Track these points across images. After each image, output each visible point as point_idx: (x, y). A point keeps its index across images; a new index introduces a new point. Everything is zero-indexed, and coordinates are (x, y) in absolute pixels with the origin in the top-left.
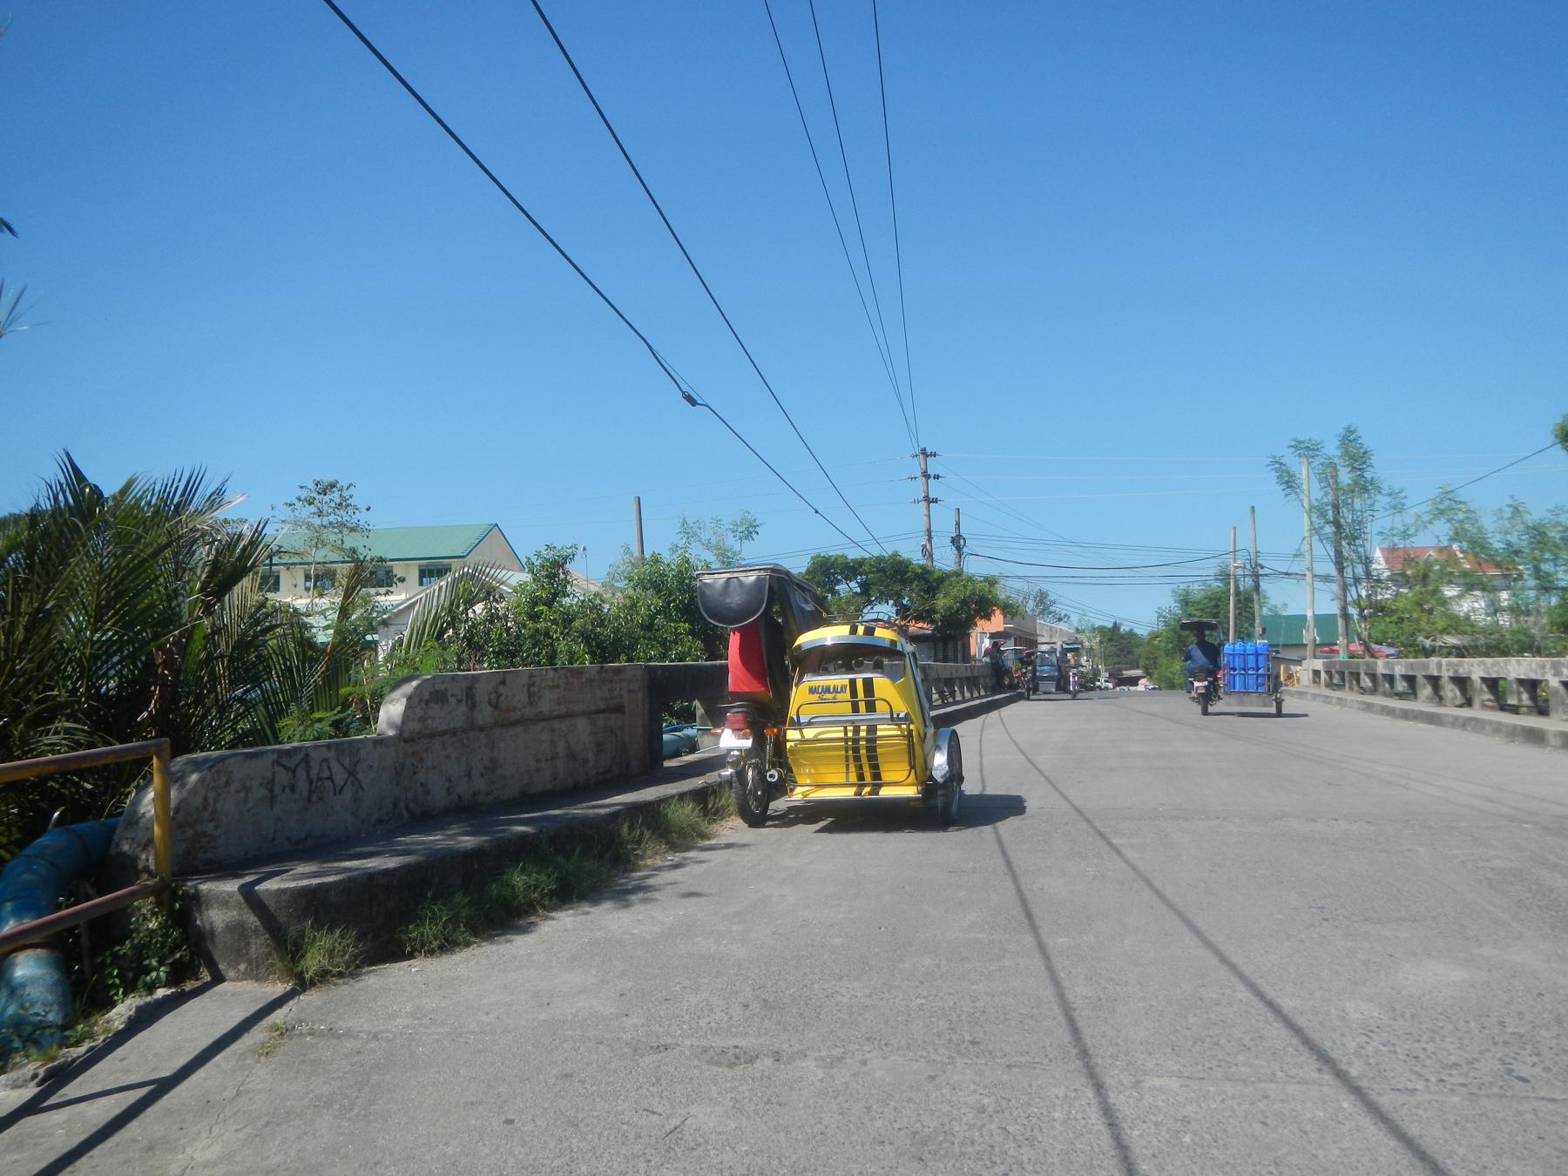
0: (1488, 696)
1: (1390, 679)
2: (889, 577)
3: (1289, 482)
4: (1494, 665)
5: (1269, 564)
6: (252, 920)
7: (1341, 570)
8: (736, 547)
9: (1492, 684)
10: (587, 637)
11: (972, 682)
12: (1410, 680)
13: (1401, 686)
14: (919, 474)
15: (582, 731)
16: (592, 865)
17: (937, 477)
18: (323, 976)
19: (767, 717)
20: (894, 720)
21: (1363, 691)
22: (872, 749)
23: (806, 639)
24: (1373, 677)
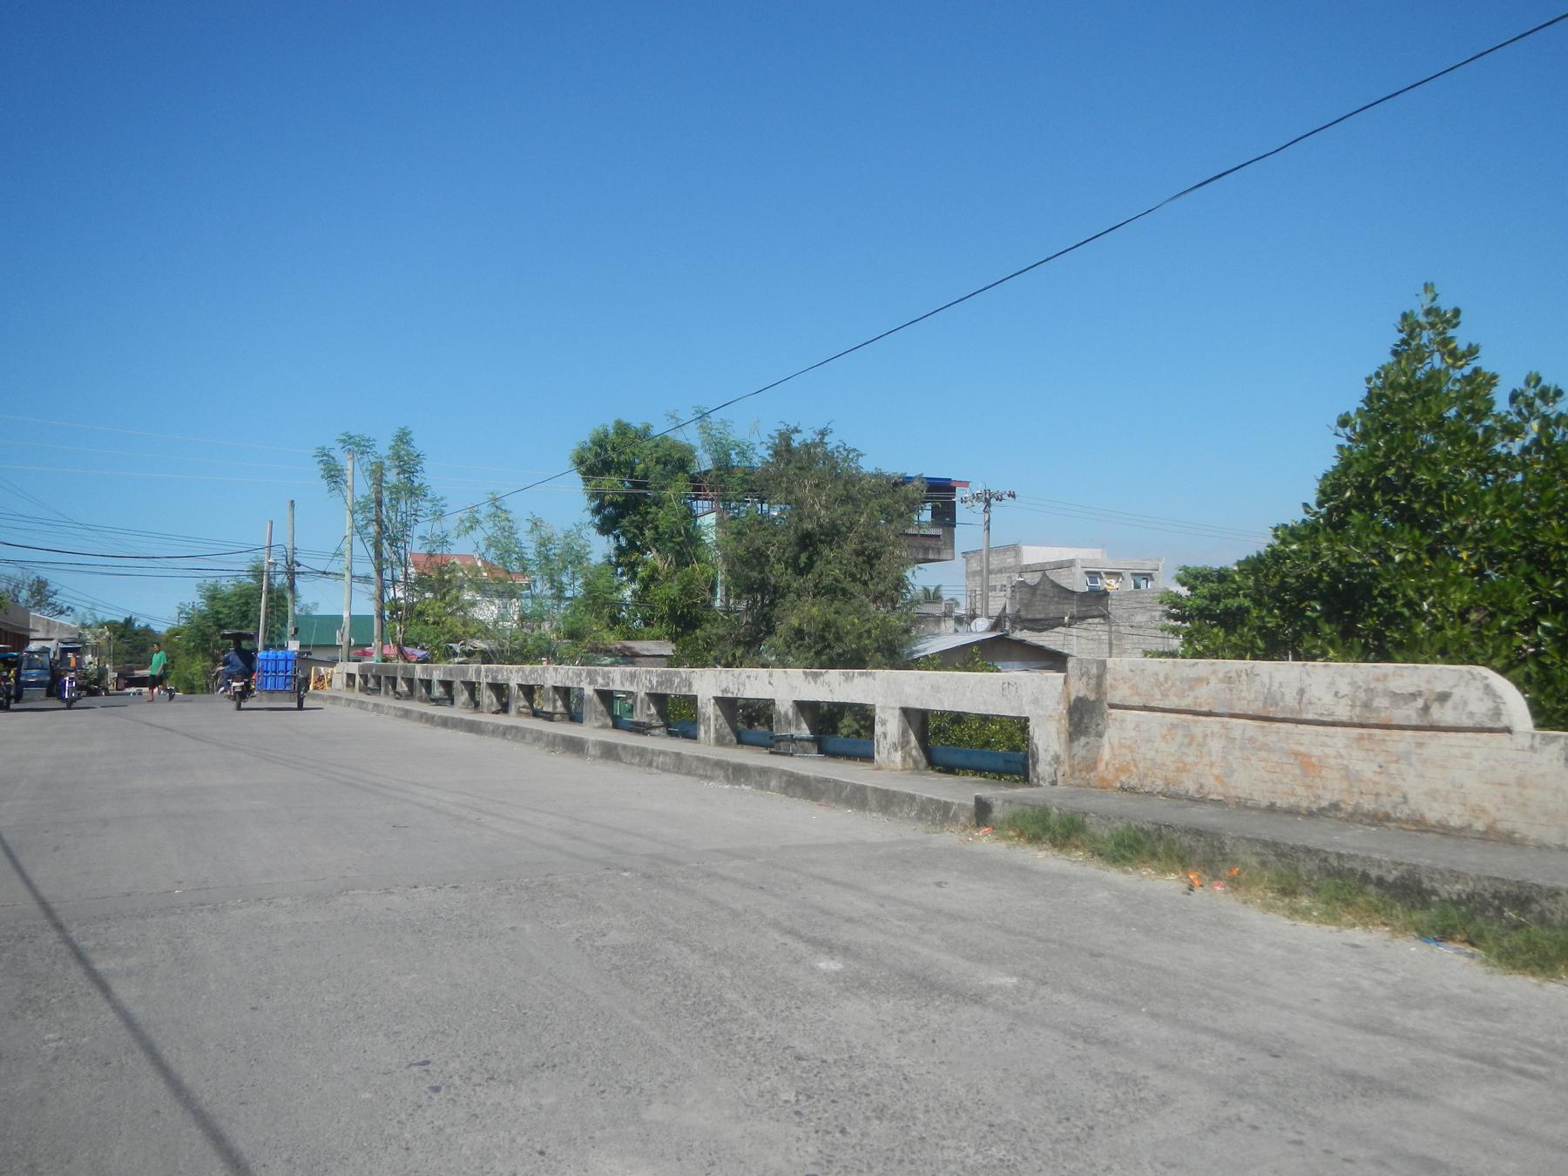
0: (523, 703)
1: (428, 684)
3: (333, 475)
4: (532, 672)
7: (380, 572)
9: (529, 691)
12: (447, 685)
13: (438, 691)
21: (398, 696)
24: (410, 682)
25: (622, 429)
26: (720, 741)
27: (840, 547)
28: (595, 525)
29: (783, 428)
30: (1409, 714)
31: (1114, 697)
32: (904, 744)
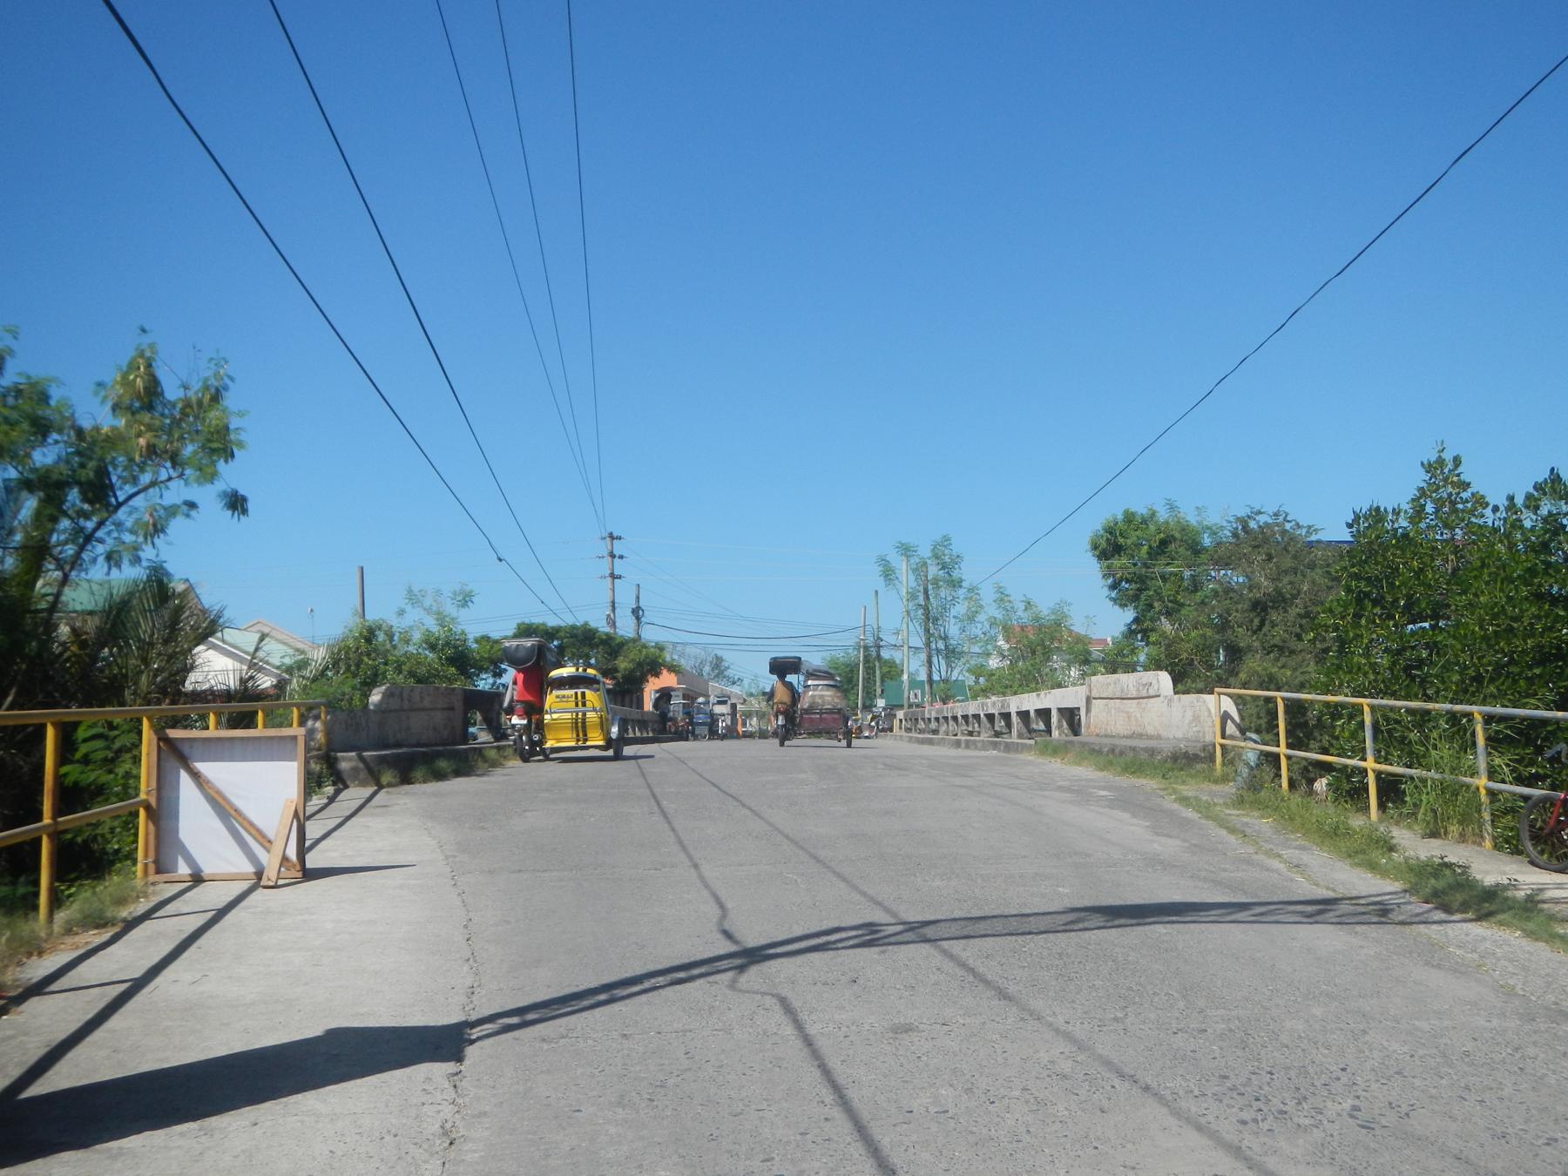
2: (583, 641)
3: (888, 574)
5: (888, 638)
6: (361, 765)
8: (454, 614)
10: (412, 674)
11: (642, 723)
12: (937, 719)
15: (439, 717)
16: (465, 763)
17: (621, 557)
18: (390, 785)
19: (534, 710)
20: (594, 710)
22: (584, 722)
23: (555, 673)
25: (1129, 517)
26: (1020, 736)
27: (1286, 611)
28: (1112, 599)
29: (1242, 513)
30: (1144, 693)
31: (1094, 694)
32: (1060, 727)
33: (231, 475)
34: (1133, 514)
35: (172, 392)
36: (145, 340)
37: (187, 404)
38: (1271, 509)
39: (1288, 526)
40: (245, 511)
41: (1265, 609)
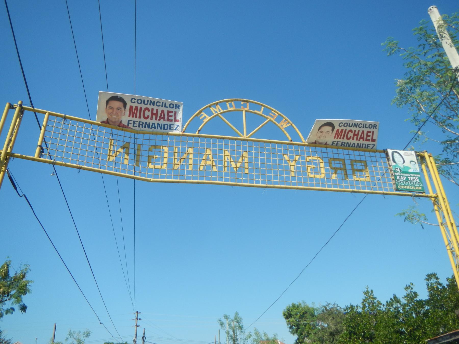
3: (222, 324)
8: (83, 340)
14: (135, 318)
17: (140, 319)
25: (294, 305)
29: (325, 304)
33: (26, 299)
34: (295, 304)
35: (12, 274)
36: (8, 259)
37: (15, 278)
38: (333, 303)
39: (338, 308)
40: (25, 311)
41: (334, 335)
